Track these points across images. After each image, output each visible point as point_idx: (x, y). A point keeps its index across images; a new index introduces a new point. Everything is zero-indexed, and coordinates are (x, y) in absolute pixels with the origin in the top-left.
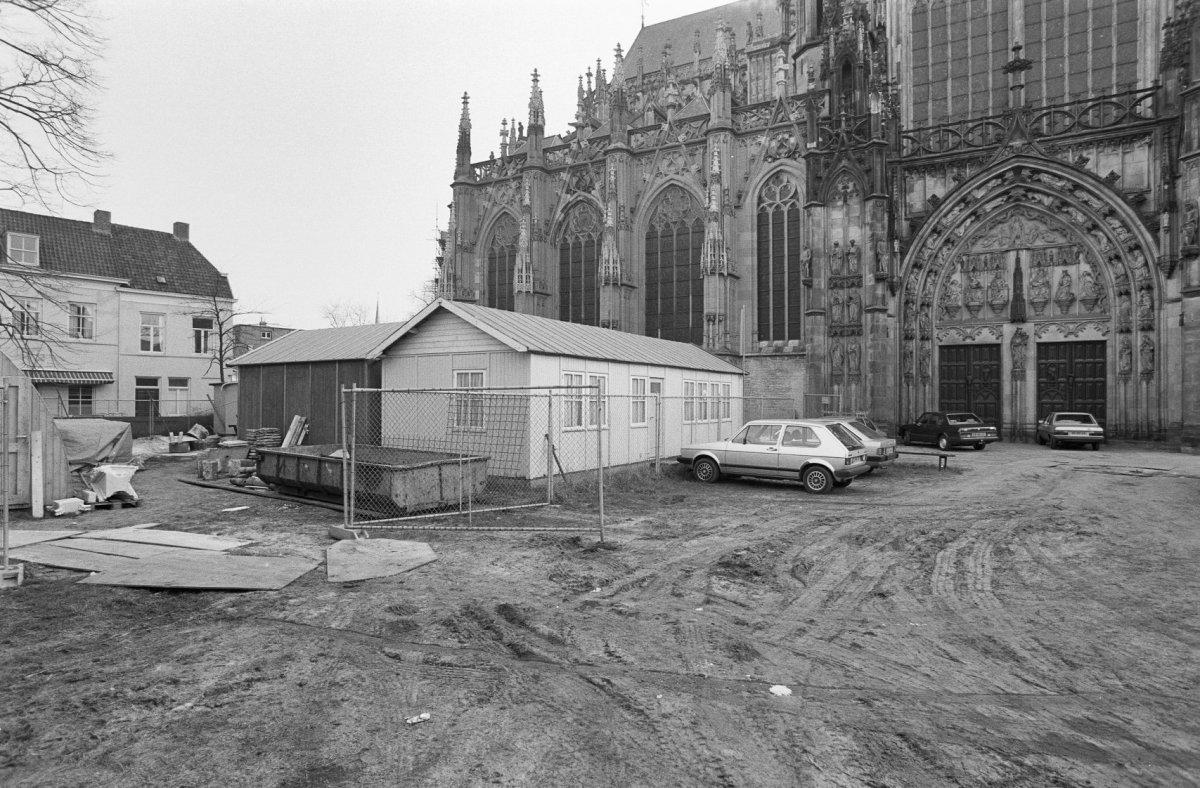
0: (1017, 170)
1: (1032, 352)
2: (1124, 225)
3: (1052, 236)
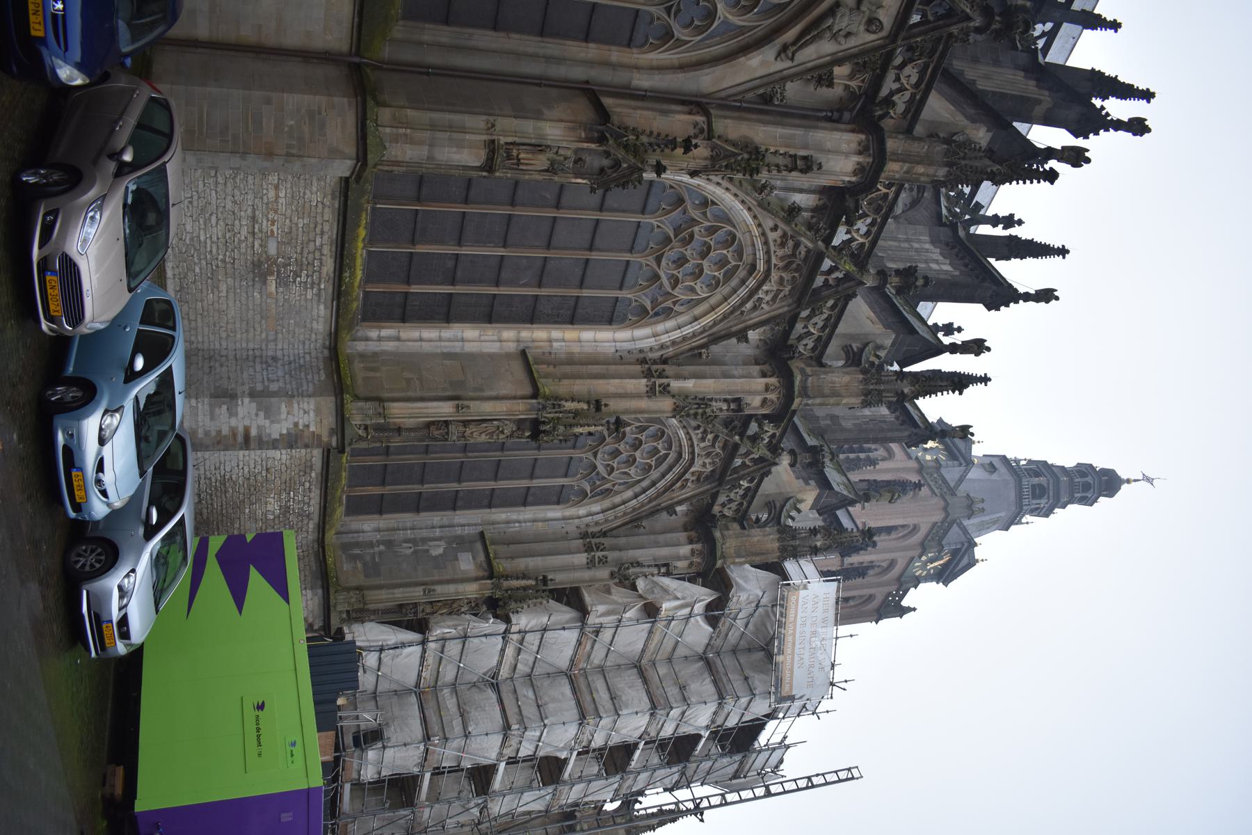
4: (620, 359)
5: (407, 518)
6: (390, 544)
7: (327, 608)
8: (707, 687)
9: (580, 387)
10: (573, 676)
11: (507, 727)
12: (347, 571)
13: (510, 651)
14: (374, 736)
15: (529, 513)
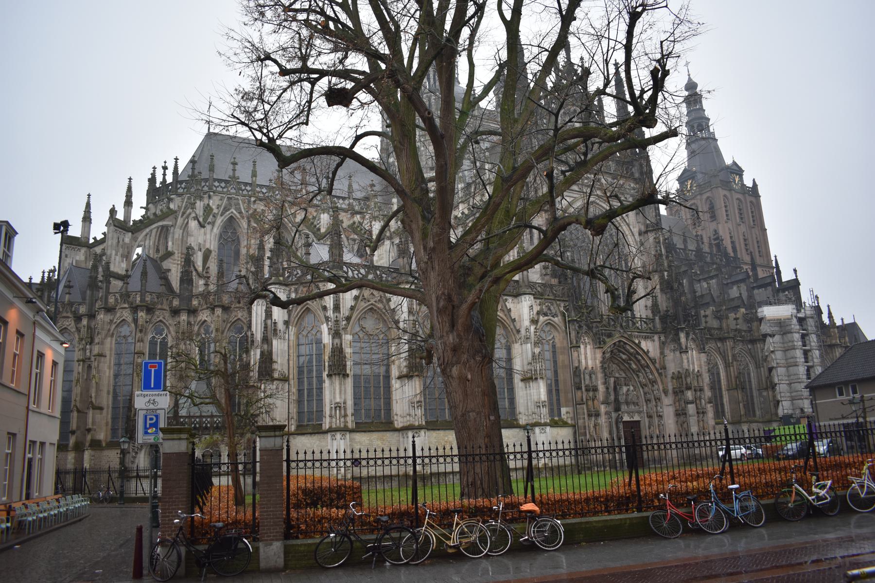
0: (620, 341)
1: (621, 426)
2: (652, 372)
3: (621, 372)
4: (726, 371)
5: (756, 406)
6: (761, 409)
7: (776, 421)
8: (789, 335)
9: (733, 380)
10: (788, 366)
11: (799, 382)
12: (768, 417)
13: (783, 382)
14: (802, 410)
15: (753, 380)
